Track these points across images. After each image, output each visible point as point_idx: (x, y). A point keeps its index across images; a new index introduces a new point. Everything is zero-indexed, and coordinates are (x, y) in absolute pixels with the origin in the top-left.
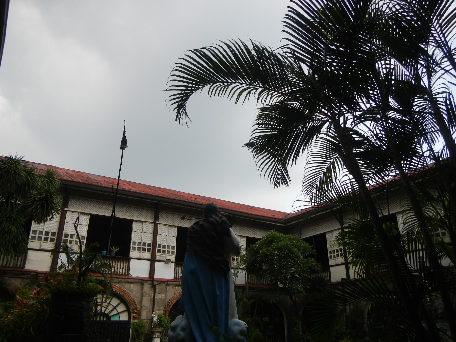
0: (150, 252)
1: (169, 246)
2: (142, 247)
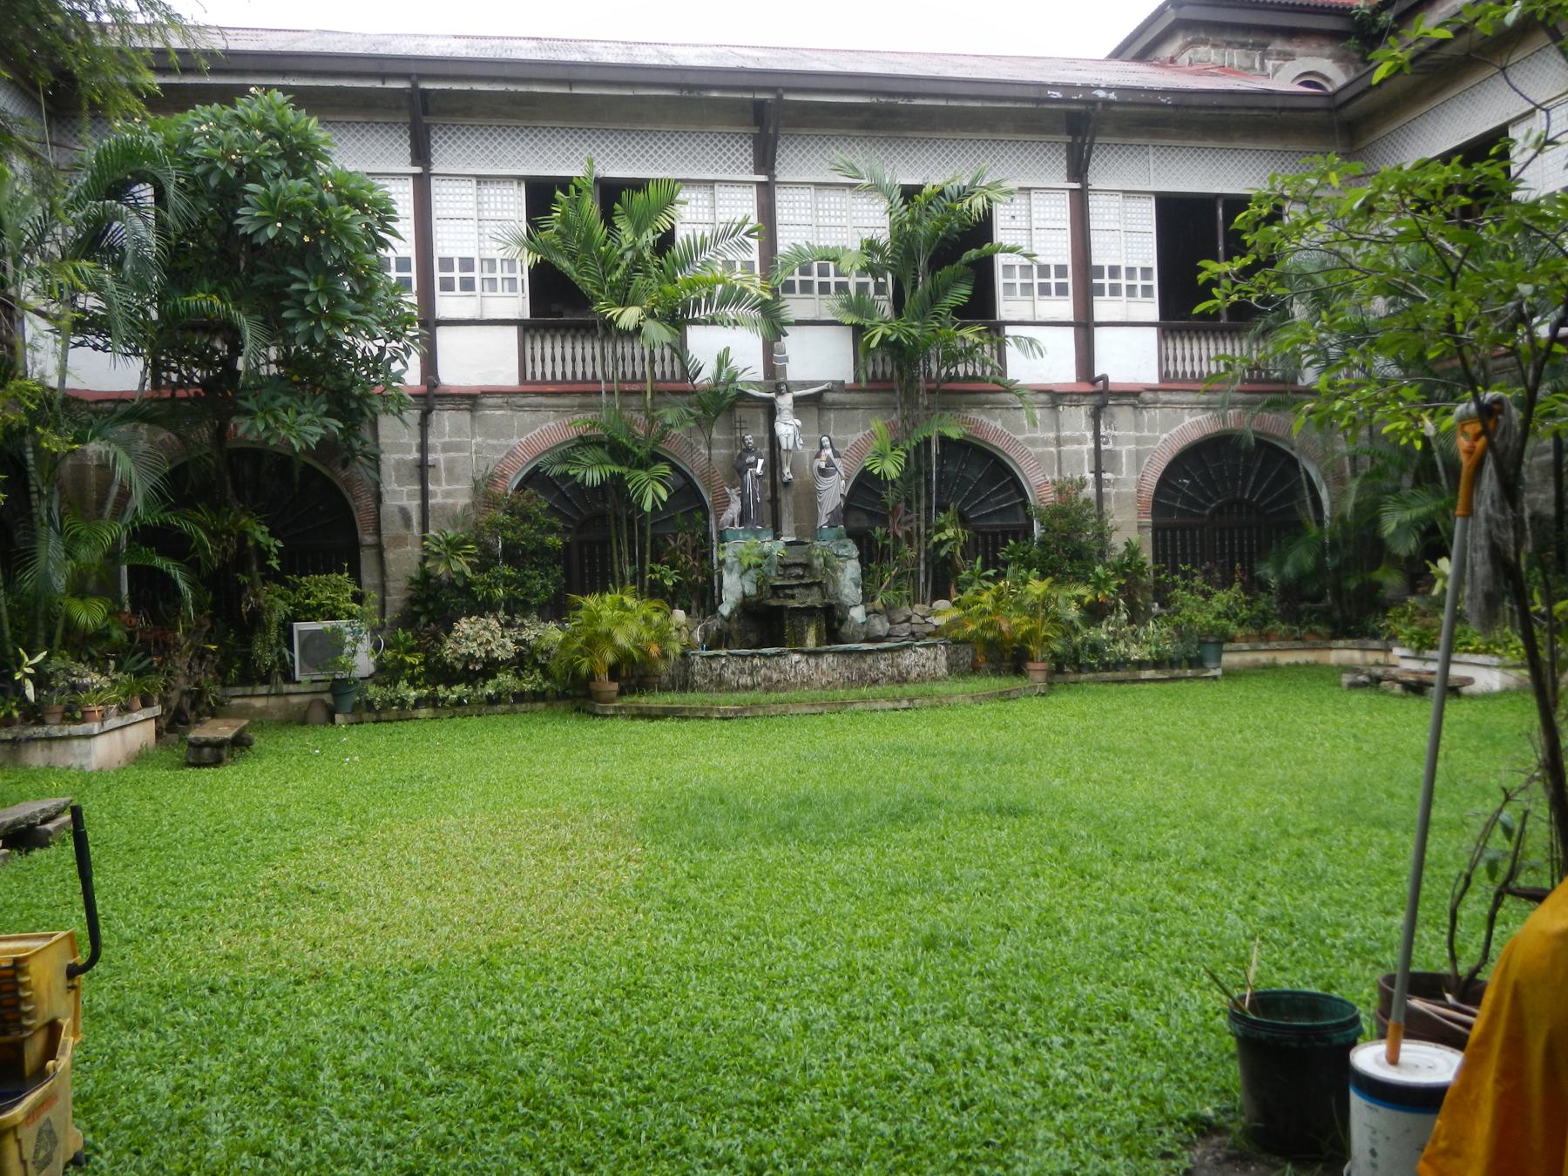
0: (1066, 294)
1: (1131, 271)
2: (1041, 280)
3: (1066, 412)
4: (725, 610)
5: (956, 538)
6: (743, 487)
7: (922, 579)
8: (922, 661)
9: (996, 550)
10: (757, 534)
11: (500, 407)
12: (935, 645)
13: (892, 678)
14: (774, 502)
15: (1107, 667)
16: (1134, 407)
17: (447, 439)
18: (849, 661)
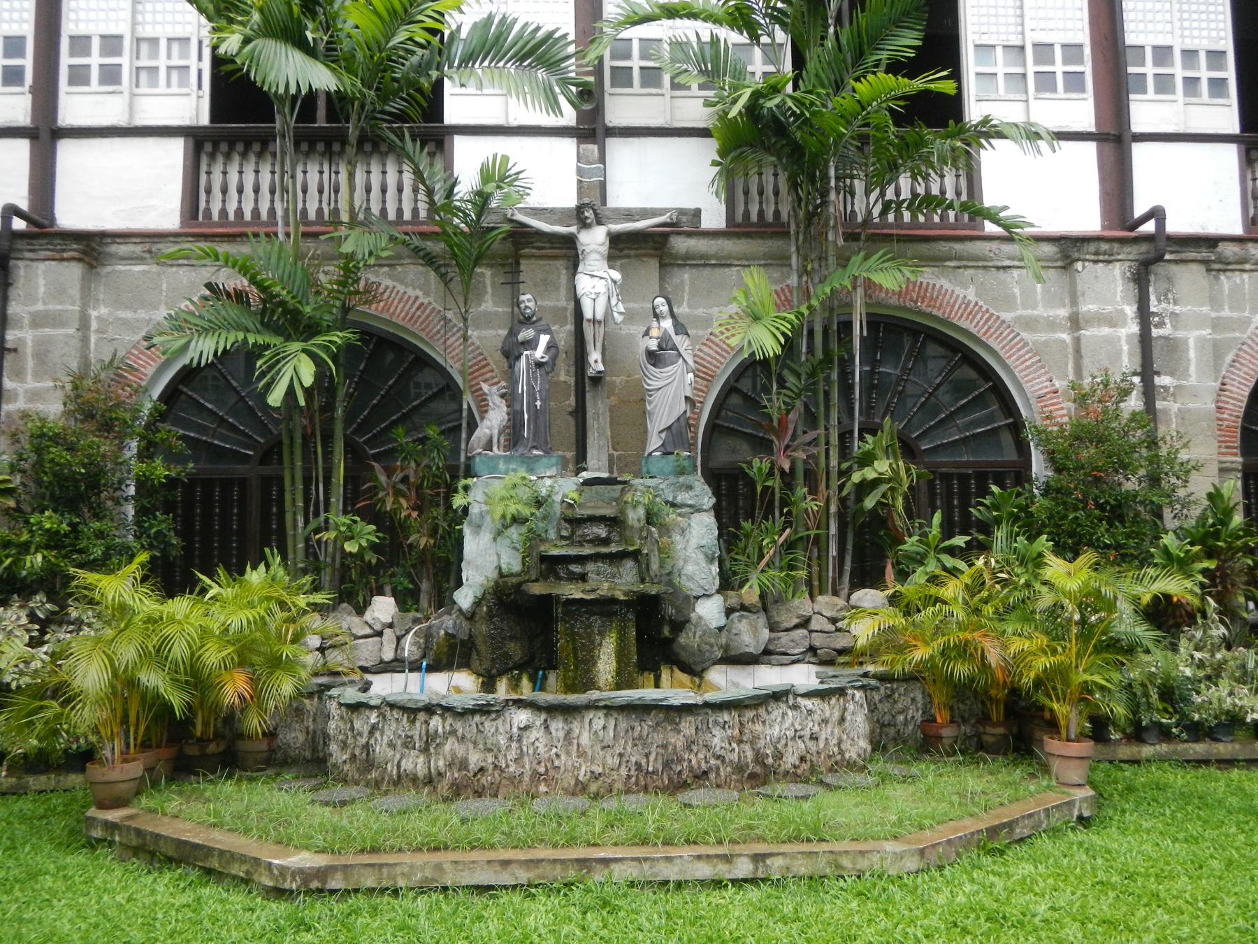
0: (1082, 89)
3: (1087, 272)
4: (464, 598)
5: (895, 478)
6: (513, 381)
7: (833, 551)
8: (811, 726)
9: (965, 505)
10: (531, 466)
11: (138, 259)
12: (841, 692)
13: (739, 768)
14: (580, 413)
15: (1197, 731)
16: (1209, 270)
17: (40, 307)
18: (643, 727)
